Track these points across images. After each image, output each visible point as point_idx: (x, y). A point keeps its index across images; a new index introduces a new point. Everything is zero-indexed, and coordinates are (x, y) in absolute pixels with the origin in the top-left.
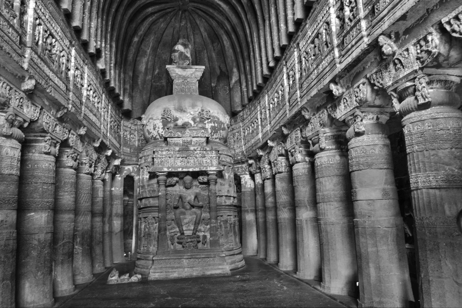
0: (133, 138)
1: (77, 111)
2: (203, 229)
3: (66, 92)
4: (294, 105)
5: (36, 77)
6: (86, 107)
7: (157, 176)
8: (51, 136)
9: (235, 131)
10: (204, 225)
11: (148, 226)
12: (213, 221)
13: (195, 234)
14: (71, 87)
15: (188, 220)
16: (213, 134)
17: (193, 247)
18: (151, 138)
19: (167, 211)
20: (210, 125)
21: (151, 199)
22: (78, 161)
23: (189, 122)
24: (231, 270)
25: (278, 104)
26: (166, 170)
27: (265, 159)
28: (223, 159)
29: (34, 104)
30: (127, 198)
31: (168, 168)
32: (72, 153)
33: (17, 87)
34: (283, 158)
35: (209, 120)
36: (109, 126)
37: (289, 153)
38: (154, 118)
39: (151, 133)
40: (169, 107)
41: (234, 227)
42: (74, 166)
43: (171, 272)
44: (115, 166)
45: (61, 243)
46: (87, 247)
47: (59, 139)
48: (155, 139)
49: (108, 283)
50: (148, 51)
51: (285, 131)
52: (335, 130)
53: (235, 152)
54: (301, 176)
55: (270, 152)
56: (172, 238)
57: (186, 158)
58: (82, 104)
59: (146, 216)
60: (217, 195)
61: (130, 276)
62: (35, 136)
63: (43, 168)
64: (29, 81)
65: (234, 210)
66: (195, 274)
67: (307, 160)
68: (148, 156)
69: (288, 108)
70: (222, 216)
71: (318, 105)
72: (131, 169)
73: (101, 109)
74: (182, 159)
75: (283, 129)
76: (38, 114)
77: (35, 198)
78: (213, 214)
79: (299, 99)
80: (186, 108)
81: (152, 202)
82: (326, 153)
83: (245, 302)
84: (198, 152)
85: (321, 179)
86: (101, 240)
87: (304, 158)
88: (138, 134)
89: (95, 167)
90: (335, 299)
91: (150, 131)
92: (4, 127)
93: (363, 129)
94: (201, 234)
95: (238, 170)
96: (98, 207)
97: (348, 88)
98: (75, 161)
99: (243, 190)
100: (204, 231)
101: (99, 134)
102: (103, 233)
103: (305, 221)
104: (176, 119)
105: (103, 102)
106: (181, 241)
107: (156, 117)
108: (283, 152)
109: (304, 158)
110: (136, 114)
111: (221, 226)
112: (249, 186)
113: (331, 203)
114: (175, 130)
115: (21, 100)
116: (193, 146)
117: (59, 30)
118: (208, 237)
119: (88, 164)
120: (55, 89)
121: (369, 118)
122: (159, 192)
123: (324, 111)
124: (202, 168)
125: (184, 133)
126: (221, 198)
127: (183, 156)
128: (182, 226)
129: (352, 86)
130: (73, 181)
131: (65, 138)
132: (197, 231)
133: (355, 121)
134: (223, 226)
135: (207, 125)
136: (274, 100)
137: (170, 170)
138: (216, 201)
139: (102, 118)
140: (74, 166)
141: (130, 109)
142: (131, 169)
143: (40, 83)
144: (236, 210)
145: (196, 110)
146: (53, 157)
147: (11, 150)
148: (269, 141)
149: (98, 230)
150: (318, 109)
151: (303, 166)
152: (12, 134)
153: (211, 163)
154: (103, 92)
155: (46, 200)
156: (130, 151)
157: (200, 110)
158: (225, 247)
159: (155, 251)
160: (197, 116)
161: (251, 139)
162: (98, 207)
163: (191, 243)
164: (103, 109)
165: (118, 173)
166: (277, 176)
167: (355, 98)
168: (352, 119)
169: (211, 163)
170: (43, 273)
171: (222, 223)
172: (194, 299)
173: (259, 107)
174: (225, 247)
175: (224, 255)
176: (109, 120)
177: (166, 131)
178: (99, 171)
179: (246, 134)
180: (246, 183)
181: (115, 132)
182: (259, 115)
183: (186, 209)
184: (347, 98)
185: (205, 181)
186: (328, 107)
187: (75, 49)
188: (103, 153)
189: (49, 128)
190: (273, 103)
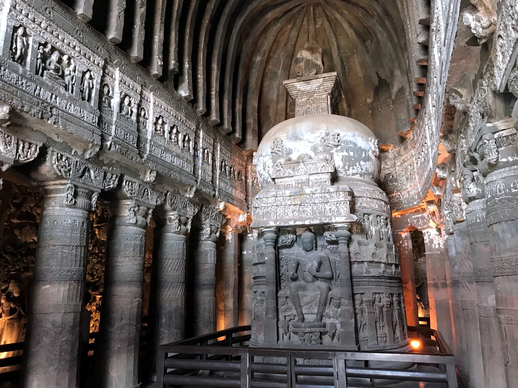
2: (331, 314)
9: (406, 164)
10: (332, 307)
16: (346, 167)
20: (341, 154)
26: (272, 224)
28: (364, 205)
31: (276, 221)
32: (133, 205)
35: (339, 148)
36: (218, 171)
38: (264, 154)
44: (241, 223)
45: (117, 325)
46: (175, 331)
48: (268, 183)
50: (279, 72)
53: (409, 194)
54: (480, 224)
62: (54, 184)
65: (388, 284)
77: (52, 266)
80: (302, 135)
82: (501, 173)
84: (318, 195)
94: (327, 321)
95: (418, 221)
103: (492, 311)
104: (290, 152)
106: (297, 330)
112: (437, 246)
117: (75, 43)
118: (339, 326)
119: (177, 221)
124: (323, 219)
126: (361, 265)
128: (301, 307)
132: (322, 317)
134: (366, 309)
137: (278, 223)
145: (318, 134)
149: (207, 306)
155: (67, 268)
157: (323, 135)
160: (319, 143)
170: (57, 368)
176: (218, 164)
179: (419, 165)
180: (431, 241)
183: (307, 282)
185: (333, 239)
187: (120, 71)
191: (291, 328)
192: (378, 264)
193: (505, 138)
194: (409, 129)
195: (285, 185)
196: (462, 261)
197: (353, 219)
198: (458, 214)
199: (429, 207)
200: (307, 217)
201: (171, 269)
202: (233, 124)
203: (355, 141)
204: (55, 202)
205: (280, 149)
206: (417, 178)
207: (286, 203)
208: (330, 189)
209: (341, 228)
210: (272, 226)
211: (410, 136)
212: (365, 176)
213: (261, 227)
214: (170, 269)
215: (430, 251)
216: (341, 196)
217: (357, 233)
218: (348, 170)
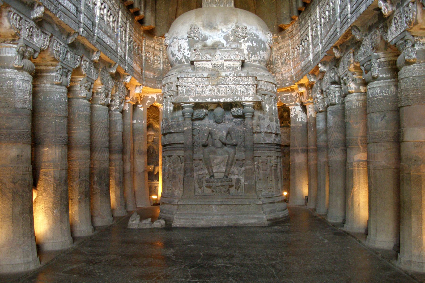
0: (157, 60)
1: (90, 35)
2: (236, 171)
3: (77, 14)
4: (344, 21)
5: (45, 3)
6: (99, 28)
7: (183, 108)
8: (62, 65)
9: (282, 51)
10: (238, 167)
11: (172, 167)
12: (249, 162)
13: (227, 177)
14: (83, 8)
15: (219, 160)
16: (250, 55)
17: (225, 192)
18: (176, 62)
19: (193, 149)
20: (247, 44)
21: (175, 135)
22: (92, 90)
23: (220, 42)
24: (268, 220)
25: (329, 19)
26: (192, 100)
27: (317, 88)
29: (43, 32)
30: (152, 133)
31: (195, 98)
32: (85, 81)
33: (26, 17)
34: (337, 86)
35: (246, 39)
36: (127, 47)
37: (342, 81)
39: (176, 55)
40: (196, 23)
41: (276, 170)
42: (88, 96)
43: (198, 219)
47: (70, 67)
48: (180, 62)
49: (128, 227)
51: (337, 54)
52: (391, 55)
53: (283, 76)
55: (322, 79)
56: (200, 181)
57: (216, 86)
58: (95, 26)
59: (170, 155)
60: (254, 131)
61: (152, 221)
63: (55, 100)
64: (38, 8)
65: (276, 150)
66: (226, 223)
67: (363, 91)
68: (172, 83)
69: (339, 25)
70: (259, 157)
71: (370, 24)
72: (156, 98)
73: (117, 28)
74: (211, 87)
75: (335, 51)
76: (48, 42)
78: (249, 154)
79: (349, 16)
80: (217, 25)
81: (177, 138)
82: (378, 83)
83: (275, 254)
84: (231, 78)
85: (372, 114)
86: (122, 180)
87: (359, 88)
88: (163, 55)
89: (112, 96)
90: (377, 253)
91: (175, 53)
92: (16, 59)
93: (414, 56)
94: (234, 177)
95: (287, 99)
96: (117, 144)
97: (398, 6)
98: (89, 90)
99: (292, 125)
100: (238, 174)
101: (115, 58)
102: (124, 173)
104: (205, 39)
105: (120, 19)
106: (211, 184)
107: (180, 36)
108: (337, 78)
109: (359, 88)
110: (158, 31)
111: (258, 168)
112: (300, 120)
113: (383, 144)
114: (204, 52)
115: (31, 30)
116: (225, 71)
118: (243, 181)
119: (104, 94)
120: (65, 13)
121: (421, 43)
122: (184, 126)
123: (376, 32)
124: (235, 98)
125: (214, 56)
126: (260, 134)
127: (213, 83)
128: (211, 167)
129: (402, 4)
130: (87, 113)
131: (77, 66)
132: (229, 173)
133: (406, 45)
135: (243, 45)
136: (325, 14)
137: (197, 100)
138: (253, 138)
139: (119, 39)
140: (88, 96)
141: (153, 25)
142: (156, 98)
143: (49, 9)
144: (280, 150)
145: (230, 26)
146: (65, 88)
147: (23, 83)
148: (320, 65)
150: (370, 29)
151: (356, 98)
152: (23, 66)
153: (247, 92)
154: (120, 8)
155: (59, 135)
156: (154, 76)
157: (234, 27)
158: (263, 193)
159: (181, 195)
160: (230, 33)
161: (301, 61)
162: (117, 144)
163: (222, 187)
164: (120, 29)
165: (139, 102)
166: (329, 109)
167: (404, 18)
168: (402, 43)
169: (247, 92)
171: (260, 165)
172: (218, 248)
173: (309, 21)
174: (263, 193)
175: (261, 202)
176: (128, 40)
177: (193, 53)
178: (117, 101)
179: (296, 54)
180: (296, 116)
181: (134, 54)
182: (310, 31)
184: (398, 18)
185: (239, 114)
186: (380, 27)
188: (121, 80)
189: (59, 56)
190: (325, 17)
191: (205, 183)
192: (270, 134)
193: (382, 63)
194: (289, 23)
195: (203, 68)
196: (333, 133)
197: (259, 99)
198: (333, 100)
199: (300, 89)
200: (222, 96)
201: (100, 136)
202: (140, 3)
203: (258, 34)
204: (47, 81)
205: (197, 35)
206: (292, 64)
207: (204, 83)
208: (241, 74)
209: (248, 106)
210: (192, 102)
211: (290, 28)
212: (262, 63)
213: (182, 103)
214: (98, 136)
215: (295, 124)
216: (250, 80)
217: (258, 110)
218: (251, 58)
